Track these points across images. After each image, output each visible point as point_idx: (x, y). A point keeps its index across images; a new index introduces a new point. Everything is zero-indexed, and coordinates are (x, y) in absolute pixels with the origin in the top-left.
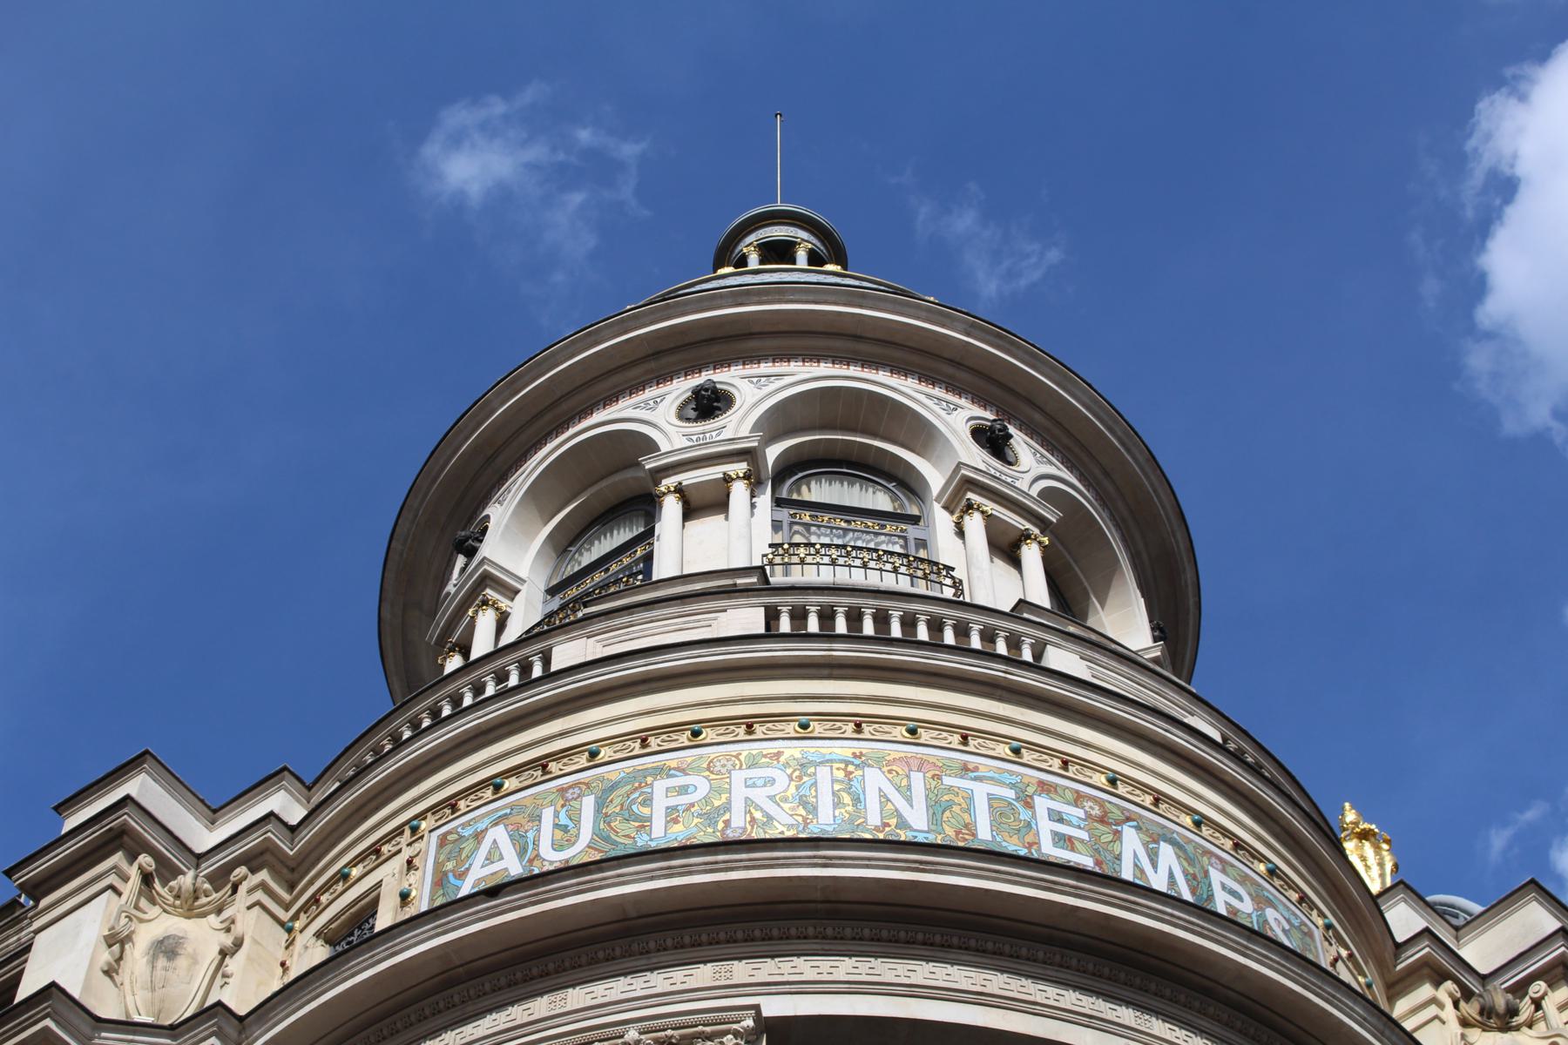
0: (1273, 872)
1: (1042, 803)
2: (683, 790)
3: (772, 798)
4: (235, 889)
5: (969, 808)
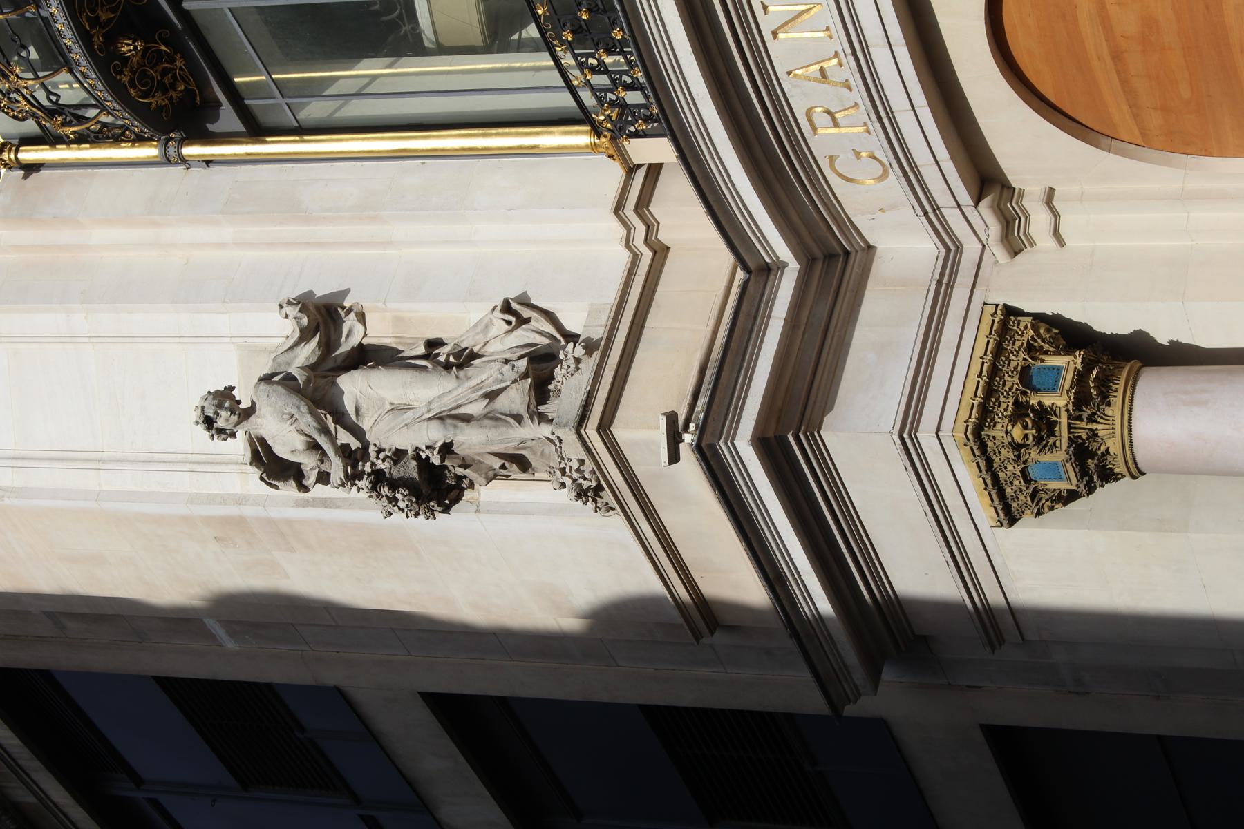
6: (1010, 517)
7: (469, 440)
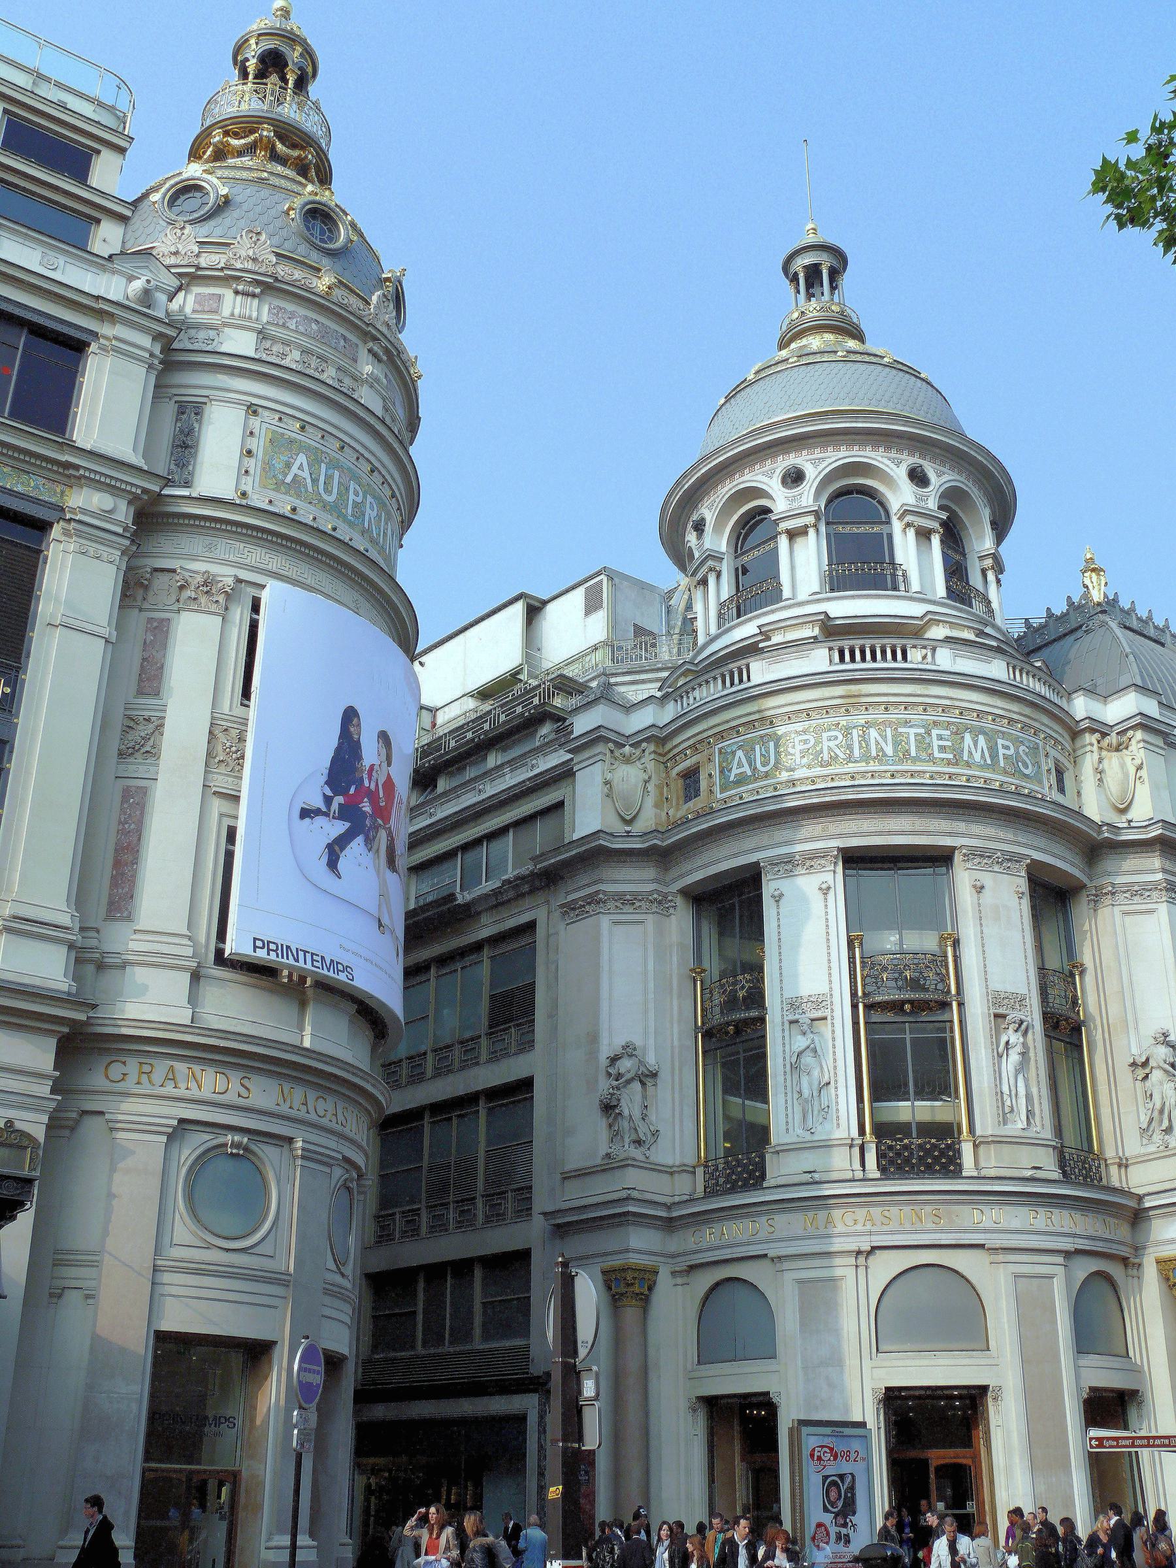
0: (1025, 726)
1: (934, 732)
2: (806, 742)
3: (837, 746)
4: (644, 751)
5: (908, 743)
6: (604, 1273)
7: (625, 1124)
